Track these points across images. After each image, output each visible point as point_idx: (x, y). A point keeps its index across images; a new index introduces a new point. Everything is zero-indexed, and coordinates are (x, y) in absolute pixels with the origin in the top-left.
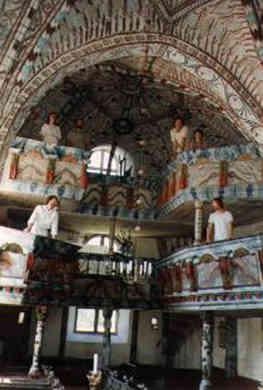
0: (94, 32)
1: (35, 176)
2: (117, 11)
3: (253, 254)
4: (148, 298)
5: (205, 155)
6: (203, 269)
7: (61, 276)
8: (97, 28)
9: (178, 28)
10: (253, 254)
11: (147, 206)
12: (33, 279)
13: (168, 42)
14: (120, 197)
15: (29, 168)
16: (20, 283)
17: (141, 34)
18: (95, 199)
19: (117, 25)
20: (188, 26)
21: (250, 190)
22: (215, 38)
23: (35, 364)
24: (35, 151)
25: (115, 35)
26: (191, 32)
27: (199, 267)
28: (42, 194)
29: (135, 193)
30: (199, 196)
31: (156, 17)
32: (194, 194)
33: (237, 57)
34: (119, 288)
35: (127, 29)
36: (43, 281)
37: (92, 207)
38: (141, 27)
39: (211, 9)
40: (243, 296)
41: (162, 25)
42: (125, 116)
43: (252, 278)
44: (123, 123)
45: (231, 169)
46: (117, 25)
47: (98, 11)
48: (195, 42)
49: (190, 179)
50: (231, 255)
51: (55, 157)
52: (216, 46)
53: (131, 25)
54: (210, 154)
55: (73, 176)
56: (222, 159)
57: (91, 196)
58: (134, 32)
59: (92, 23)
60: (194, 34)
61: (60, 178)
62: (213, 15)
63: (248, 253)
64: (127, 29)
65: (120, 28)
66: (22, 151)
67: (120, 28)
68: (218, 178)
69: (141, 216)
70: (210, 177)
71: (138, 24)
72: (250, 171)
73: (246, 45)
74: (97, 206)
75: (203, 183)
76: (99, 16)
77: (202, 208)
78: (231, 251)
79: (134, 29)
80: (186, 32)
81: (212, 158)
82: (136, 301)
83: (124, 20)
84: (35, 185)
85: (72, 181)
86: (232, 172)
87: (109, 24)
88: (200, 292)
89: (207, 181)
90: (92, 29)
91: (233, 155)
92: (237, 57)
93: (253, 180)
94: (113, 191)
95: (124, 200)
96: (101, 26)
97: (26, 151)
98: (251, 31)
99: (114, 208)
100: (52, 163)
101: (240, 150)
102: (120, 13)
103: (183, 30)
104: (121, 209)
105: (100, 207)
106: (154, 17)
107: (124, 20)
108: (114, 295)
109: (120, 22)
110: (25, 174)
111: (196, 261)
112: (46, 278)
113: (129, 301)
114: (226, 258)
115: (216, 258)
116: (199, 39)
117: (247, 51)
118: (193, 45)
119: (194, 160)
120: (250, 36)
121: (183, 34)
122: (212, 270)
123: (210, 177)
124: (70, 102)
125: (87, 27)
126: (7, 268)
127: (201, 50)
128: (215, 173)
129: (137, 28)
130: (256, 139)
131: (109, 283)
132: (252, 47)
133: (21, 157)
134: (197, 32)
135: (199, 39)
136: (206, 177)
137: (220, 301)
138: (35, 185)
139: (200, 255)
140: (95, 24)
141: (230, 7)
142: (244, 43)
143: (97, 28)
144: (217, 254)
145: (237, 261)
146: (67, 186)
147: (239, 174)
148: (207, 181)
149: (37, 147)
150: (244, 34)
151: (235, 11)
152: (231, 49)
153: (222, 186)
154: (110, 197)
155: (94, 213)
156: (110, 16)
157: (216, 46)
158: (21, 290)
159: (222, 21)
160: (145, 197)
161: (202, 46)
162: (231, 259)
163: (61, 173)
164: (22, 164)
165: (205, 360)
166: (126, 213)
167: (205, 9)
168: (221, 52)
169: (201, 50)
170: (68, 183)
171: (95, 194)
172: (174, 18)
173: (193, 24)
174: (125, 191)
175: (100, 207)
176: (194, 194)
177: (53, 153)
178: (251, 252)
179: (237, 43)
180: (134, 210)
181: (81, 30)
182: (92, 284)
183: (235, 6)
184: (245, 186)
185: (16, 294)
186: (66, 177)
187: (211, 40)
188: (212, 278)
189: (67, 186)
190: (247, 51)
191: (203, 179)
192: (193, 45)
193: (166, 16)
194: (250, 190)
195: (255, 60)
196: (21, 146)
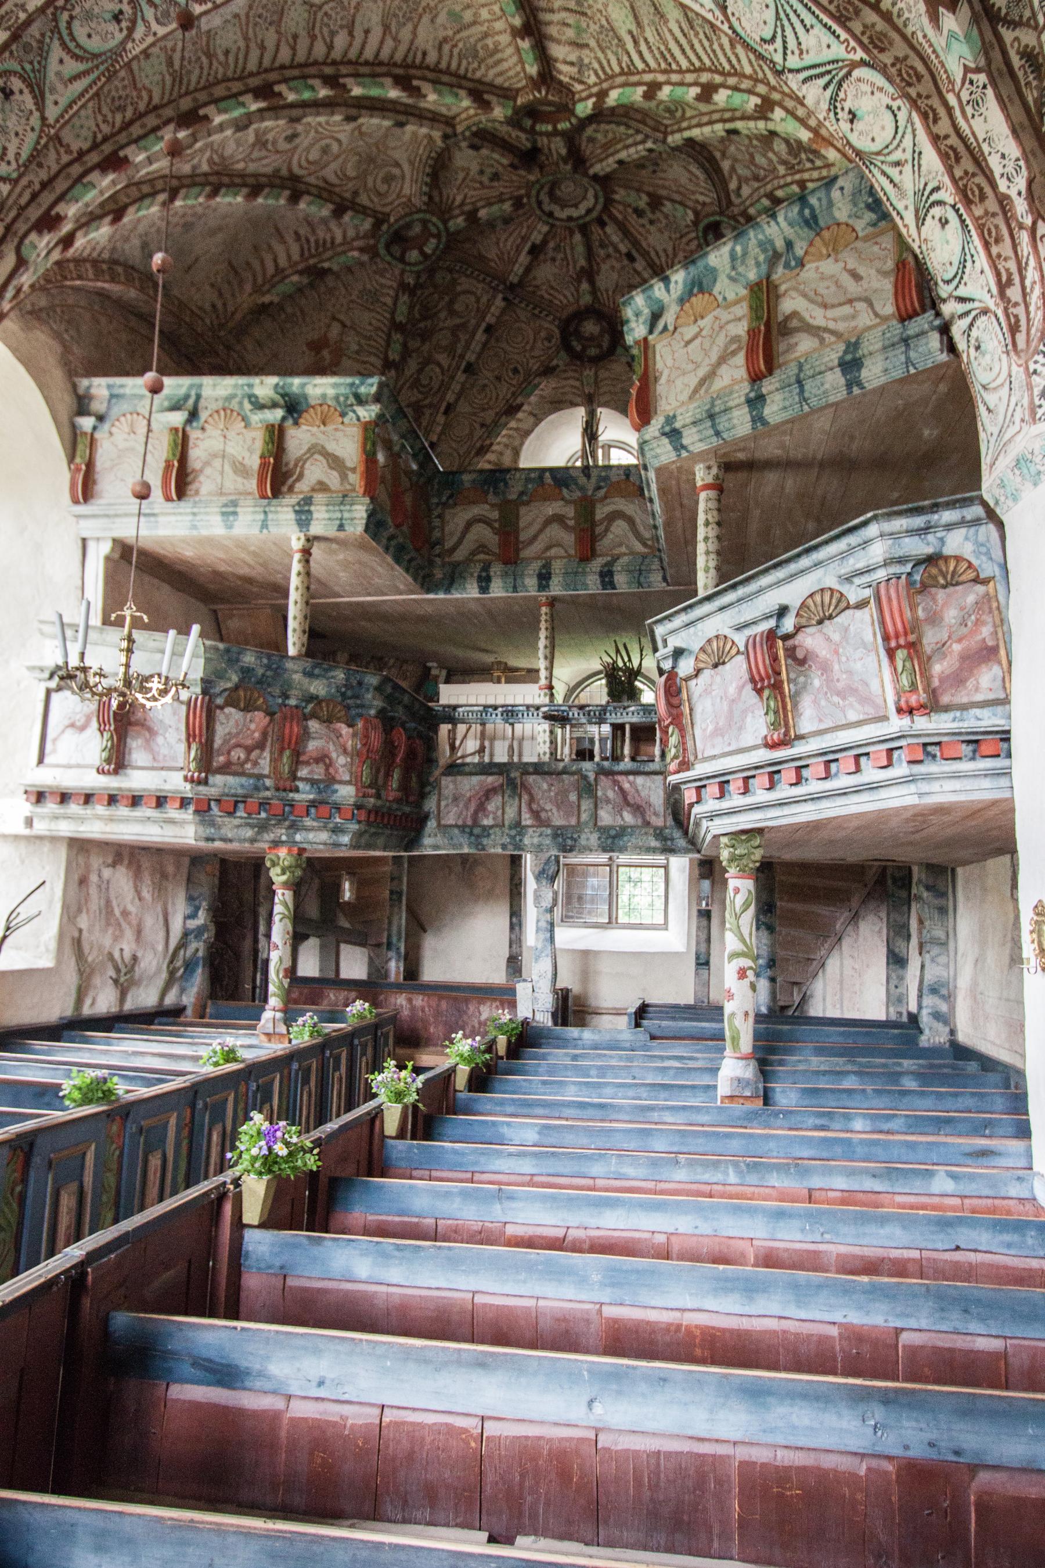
1: (233, 482)
3: (862, 605)
4: (658, 822)
5: (699, 287)
6: (707, 691)
7: (323, 759)
10: (862, 605)
11: (639, 547)
12: (225, 769)
14: (555, 531)
15: (217, 463)
16: (176, 783)
18: (482, 548)
21: (851, 365)
23: (273, 1001)
24: (226, 410)
27: (696, 687)
28: (255, 531)
29: (601, 512)
30: (690, 438)
32: (673, 435)
34: (573, 797)
36: (260, 777)
37: (476, 570)
40: (829, 759)
42: (587, 299)
43: (866, 700)
44: (590, 327)
45: (788, 305)
49: (661, 388)
50: (788, 624)
51: (279, 413)
54: (713, 272)
55: (335, 462)
56: (752, 275)
57: (471, 536)
61: (301, 476)
63: (842, 605)
66: (193, 415)
68: (740, 359)
69: (621, 579)
70: (722, 360)
72: (853, 288)
74: (486, 568)
75: (696, 391)
77: (718, 487)
78: (782, 611)
81: (726, 288)
82: (622, 831)
84: (230, 511)
85: (333, 479)
86: (795, 314)
88: (700, 769)
89: (712, 374)
91: (789, 245)
93: (865, 319)
94: (531, 517)
95: (569, 539)
97: (204, 415)
99: (536, 566)
100: (276, 436)
101: (811, 222)
104: (557, 566)
105: (496, 569)
108: (558, 820)
110: (205, 484)
111: (685, 667)
112: (265, 765)
113: (604, 830)
114: (771, 636)
115: (740, 639)
119: (669, 318)
122: (732, 690)
123: (722, 360)
124: (403, 287)
126: (148, 746)
128: (735, 339)
130: (853, 139)
131: (540, 785)
133: (194, 434)
136: (714, 357)
137: (760, 795)
138: (230, 511)
139: (696, 647)
144: (739, 628)
145: (810, 640)
146: (319, 498)
147: (817, 317)
148: (712, 374)
149: (229, 398)
153: (756, 378)
154: (523, 536)
155: (484, 589)
158: (184, 803)
160: (630, 521)
162: (786, 637)
163: (301, 461)
164: (197, 454)
165: (731, 997)
166: (573, 577)
170: (322, 487)
171: (482, 533)
174: (570, 511)
175: (496, 569)
176: (673, 435)
177: (274, 405)
178: (853, 594)
180: (597, 564)
182: (489, 793)
184: (833, 354)
185: (172, 812)
186: (315, 472)
188: (733, 723)
189: (319, 498)
191: (701, 372)
194: (851, 365)
196: (191, 402)
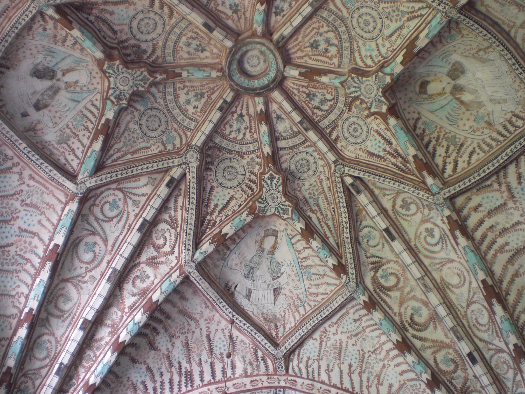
0: (167, 386)
2: (199, 355)
8: (171, 382)
9: (295, 362)
13: (282, 384)
17: (239, 381)
19: (202, 373)
20: (309, 359)
22: (350, 366)
25: (199, 387)
26: (315, 366)
31: (260, 354)
33: (391, 386)
35: (219, 376)
38: (239, 371)
39: (333, 330)
41: (269, 362)
46: (202, 373)
47: (168, 357)
48: (324, 377)
52: (356, 377)
53: (224, 371)
58: (230, 379)
59: (162, 375)
60: (319, 367)
62: (337, 337)
64: (219, 376)
65: (207, 377)
67: (207, 377)
71: (233, 367)
73: (396, 366)
76: (171, 365)
79: (229, 373)
80: (307, 367)
83: (212, 365)
87: (189, 375)
90: (162, 383)
92: (391, 386)
96: (176, 378)
98: (394, 344)
102: (205, 356)
103: (302, 366)
106: (256, 353)
107: (212, 365)
109: (207, 369)
116: (328, 371)
117: (401, 374)
118: (323, 383)
120: (396, 352)
121: (304, 371)
125: (154, 381)
127: (335, 386)
129: (234, 374)
132: (405, 367)
134: (324, 364)
135: (328, 371)
140: (166, 377)
141: (355, 321)
142: (392, 364)
143: (171, 382)
150: (388, 352)
151: (364, 324)
152: (378, 377)
156: (189, 362)
157: (356, 377)
159: (353, 341)
161: (336, 380)
167: (325, 332)
168: (365, 384)
169: (335, 386)
172: (283, 350)
173: (314, 355)
179: (384, 366)
181: (145, 387)
183: (361, 317)
187: (345, 368)
190: (401, 374)
192: (323, 383)
193: (271, 349)
195: (417, 383)
